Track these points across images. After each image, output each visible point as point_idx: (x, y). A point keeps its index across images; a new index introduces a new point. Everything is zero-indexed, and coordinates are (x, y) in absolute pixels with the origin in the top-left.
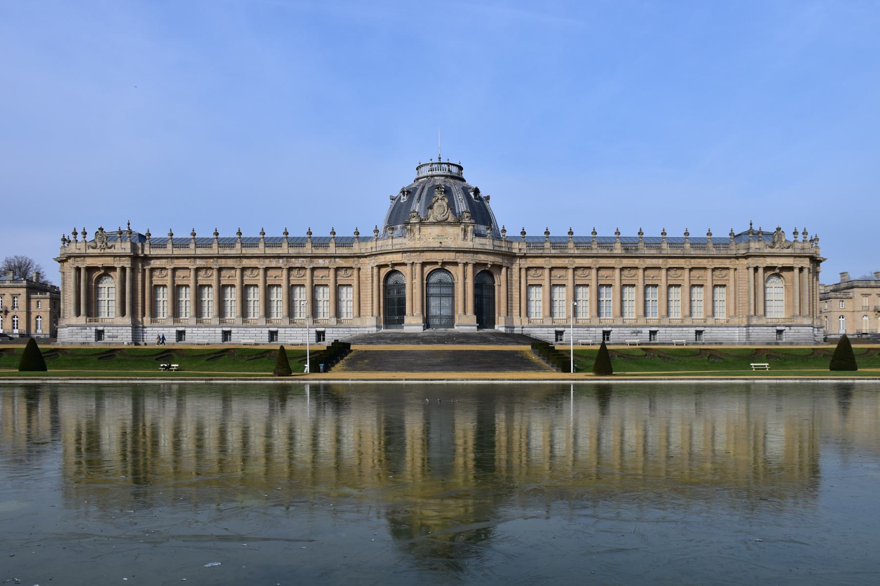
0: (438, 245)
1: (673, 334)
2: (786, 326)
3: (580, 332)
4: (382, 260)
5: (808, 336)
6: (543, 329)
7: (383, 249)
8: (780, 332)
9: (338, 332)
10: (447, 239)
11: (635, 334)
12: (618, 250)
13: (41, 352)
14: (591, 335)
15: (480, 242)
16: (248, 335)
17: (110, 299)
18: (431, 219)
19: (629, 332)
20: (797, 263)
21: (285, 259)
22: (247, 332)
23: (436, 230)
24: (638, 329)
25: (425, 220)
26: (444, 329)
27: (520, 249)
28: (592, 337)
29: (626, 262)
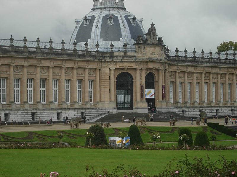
4: (120, 65)
11: (211, 112)
16: (46, 115)
19: (209, 110)
22: (46, 113)
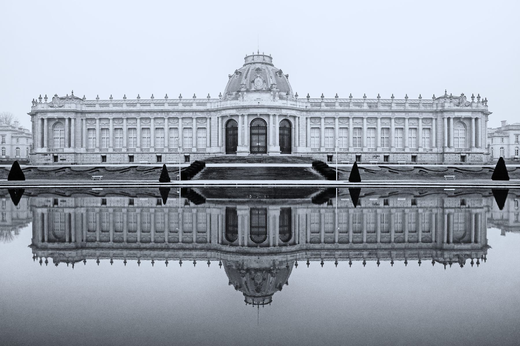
0: (257, 104)
1: (398, 158)
2: (467, 154)
3: (342, 156)
4: (224, 113)
5: (479, 160)
6: (320, 154)
7: (224, 106)
8: (463, 158)
9: (197, 156)
10: (263, 100)
12: (365, 107)
13: (21, 168)
14: (349, 158)
15: (283, 102)
17: (61, 137)
18: (253, 89)
19: (372, 156)
20: (474, 116)
21: (166, 113)
22: (143, 156)
23: (256, 95)
24: (377, 155)
25: (250, 89)
26: (261, 154)
27: (306, 107)
28: (349, 159)
29: (370, 115)
